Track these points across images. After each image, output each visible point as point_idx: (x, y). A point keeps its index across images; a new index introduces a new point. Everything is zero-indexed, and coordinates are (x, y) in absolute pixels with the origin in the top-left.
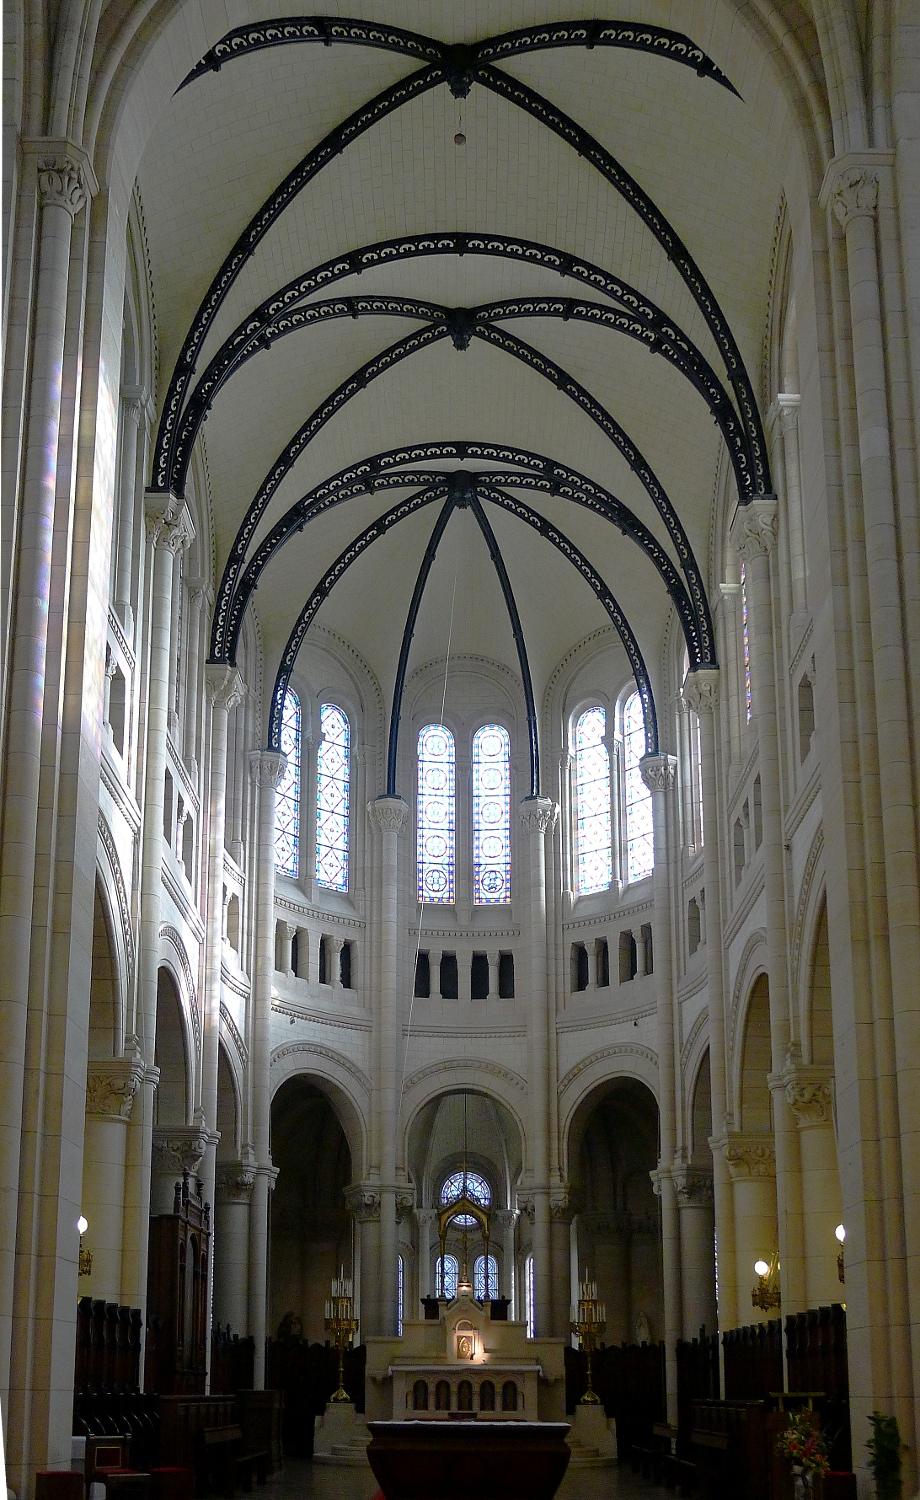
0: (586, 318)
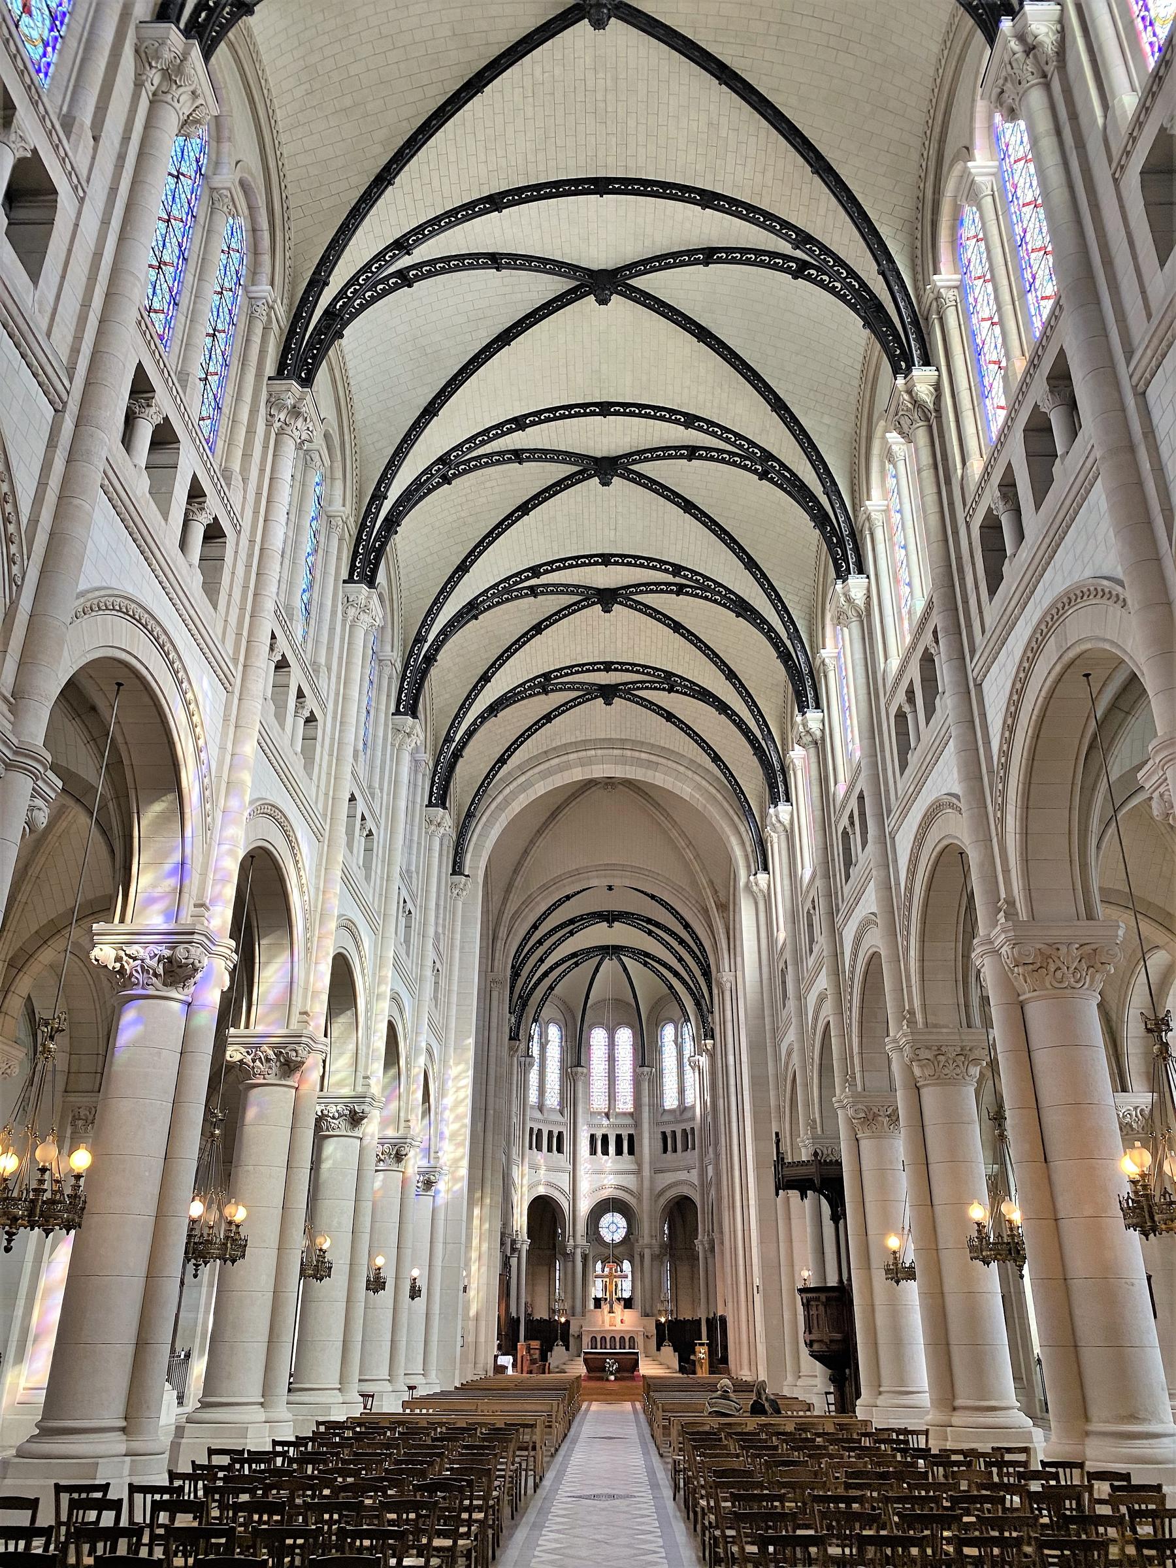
0: (691, 595)
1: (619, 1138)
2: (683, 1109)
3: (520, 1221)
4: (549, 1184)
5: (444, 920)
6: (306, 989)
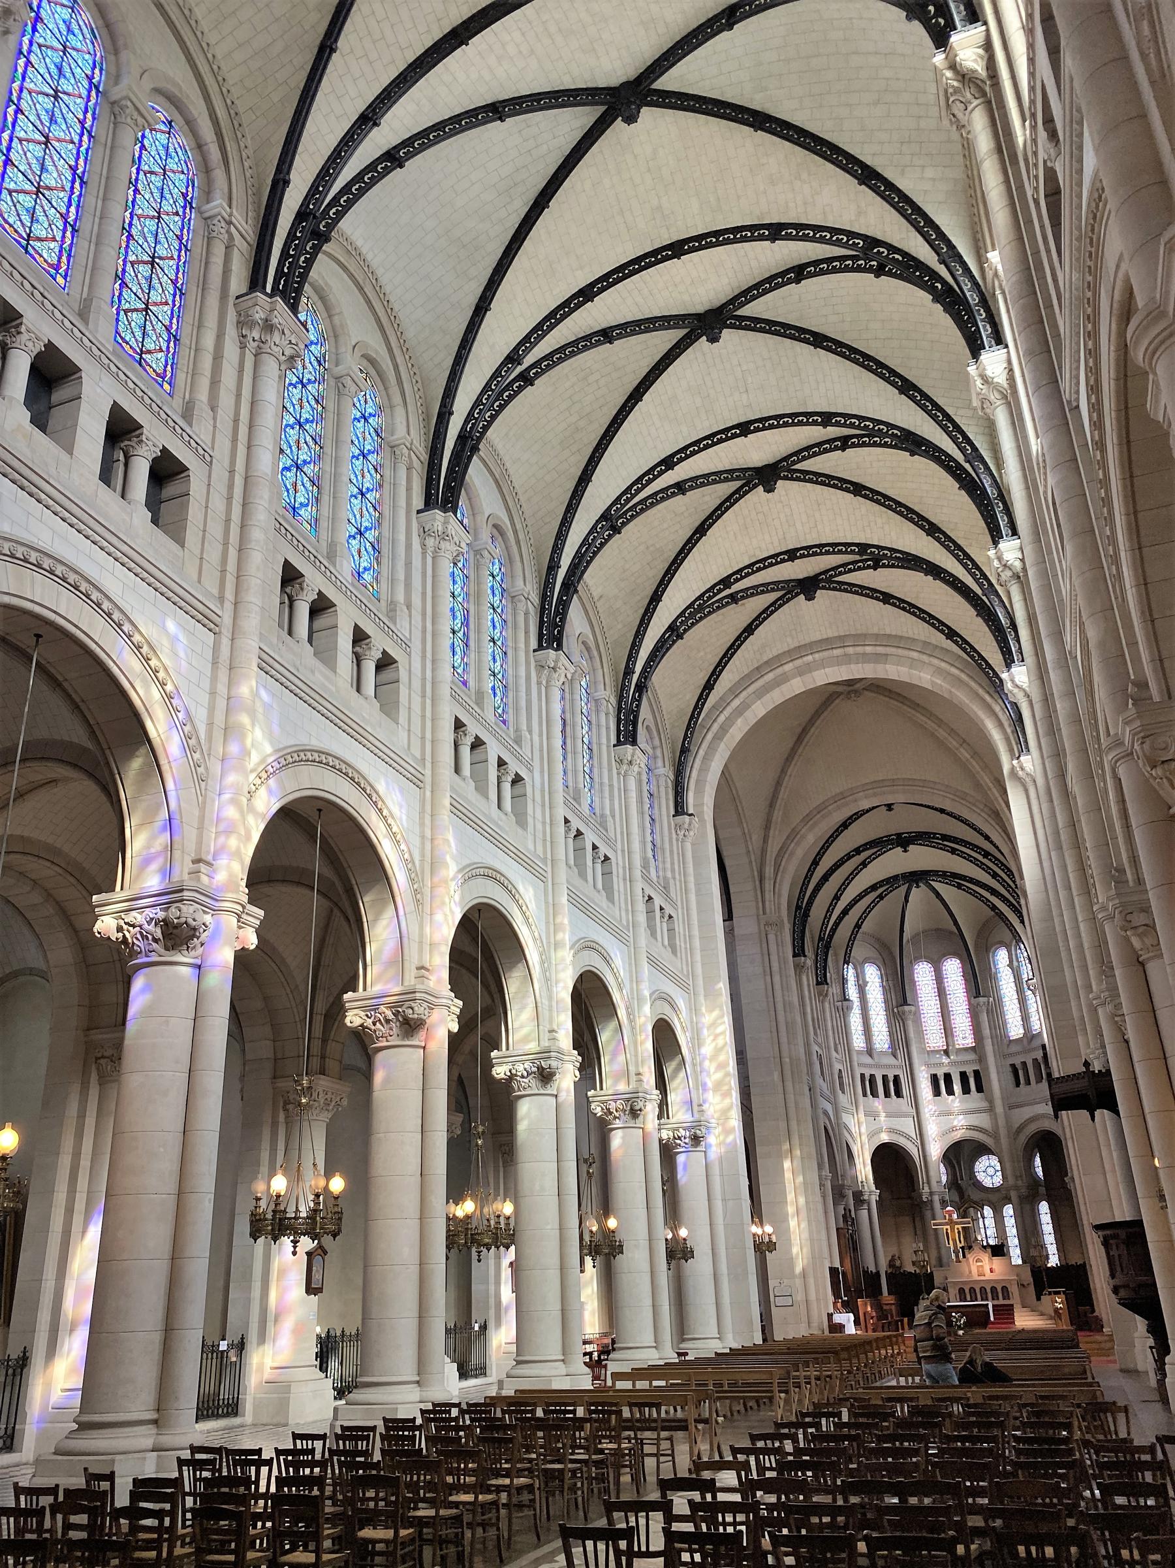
1: (964, 1076)
2: (1030, 1036)
3: (864, 1170)
4: (891, 1131)
5: (672, 864)
6: (421, 942)
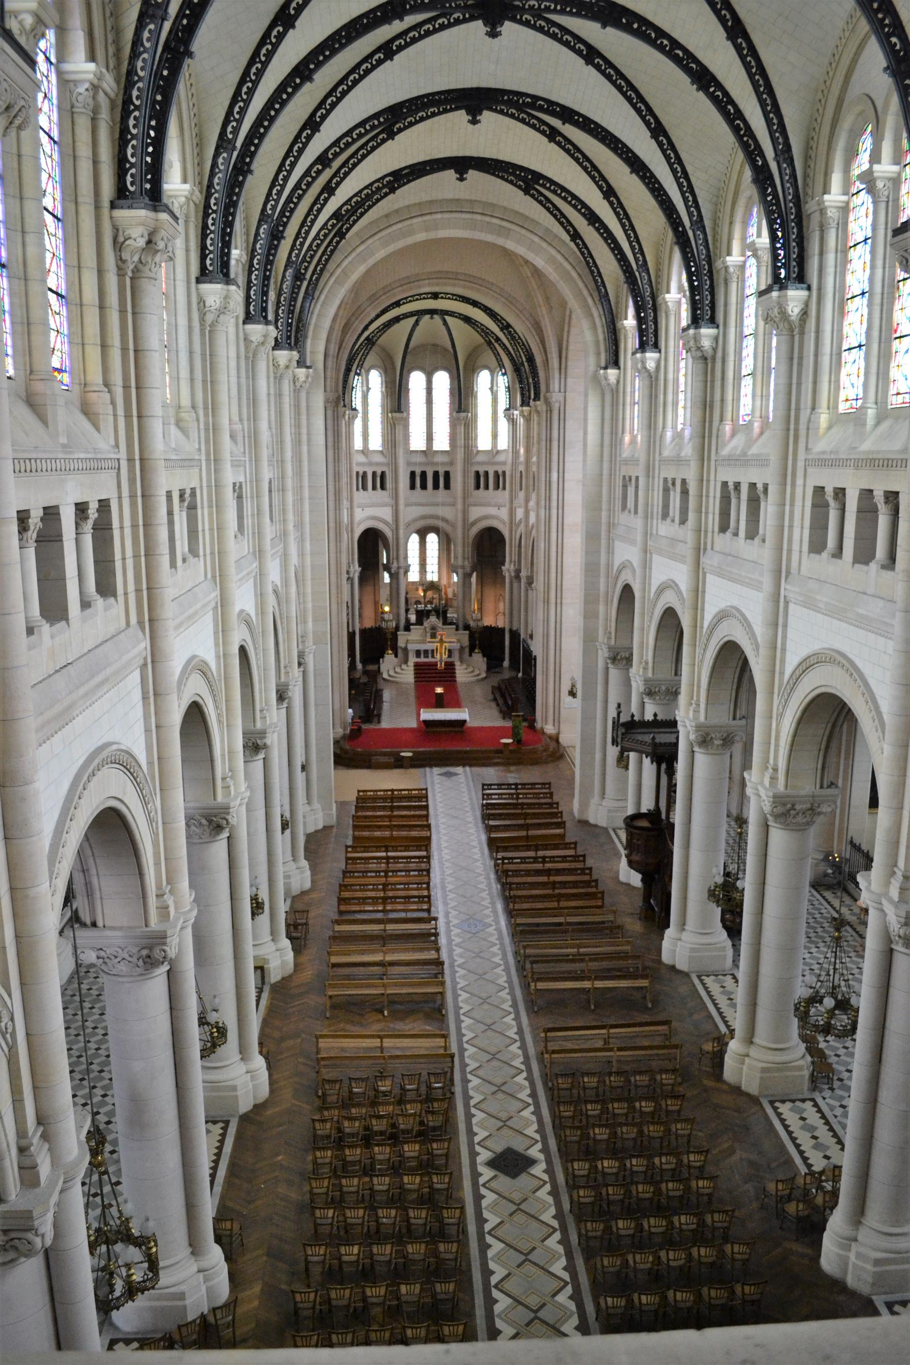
1: (436, 474)
